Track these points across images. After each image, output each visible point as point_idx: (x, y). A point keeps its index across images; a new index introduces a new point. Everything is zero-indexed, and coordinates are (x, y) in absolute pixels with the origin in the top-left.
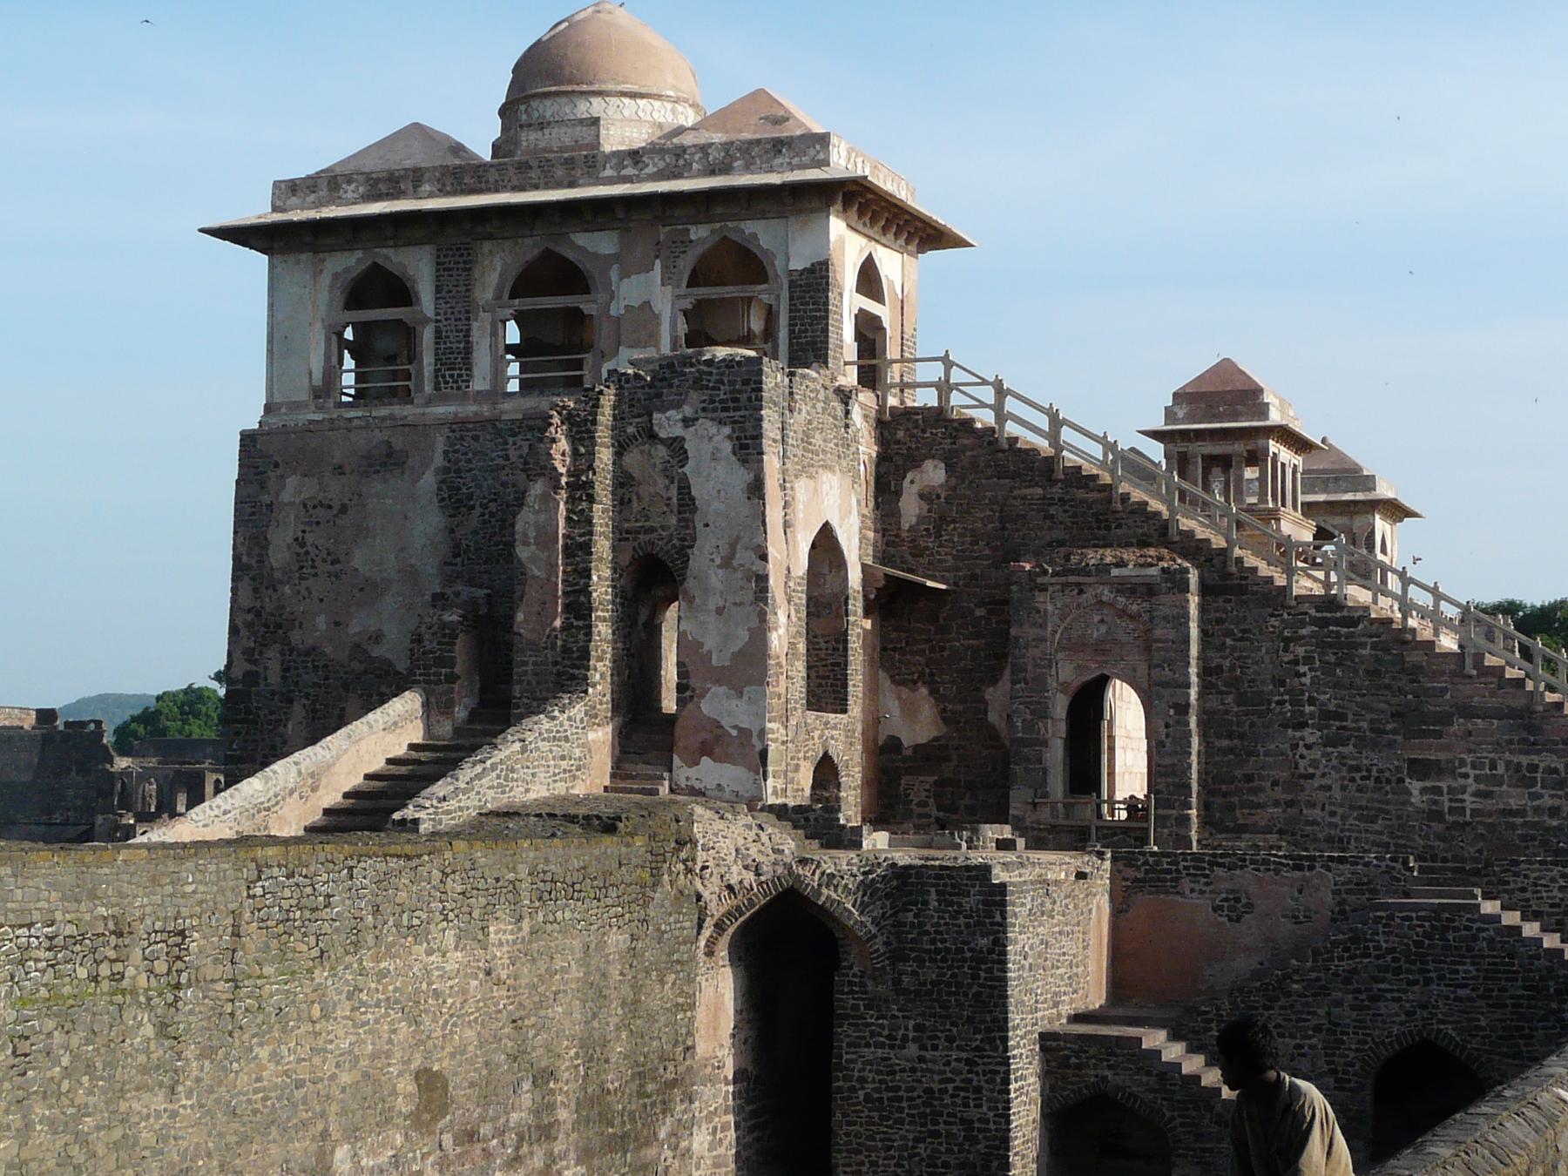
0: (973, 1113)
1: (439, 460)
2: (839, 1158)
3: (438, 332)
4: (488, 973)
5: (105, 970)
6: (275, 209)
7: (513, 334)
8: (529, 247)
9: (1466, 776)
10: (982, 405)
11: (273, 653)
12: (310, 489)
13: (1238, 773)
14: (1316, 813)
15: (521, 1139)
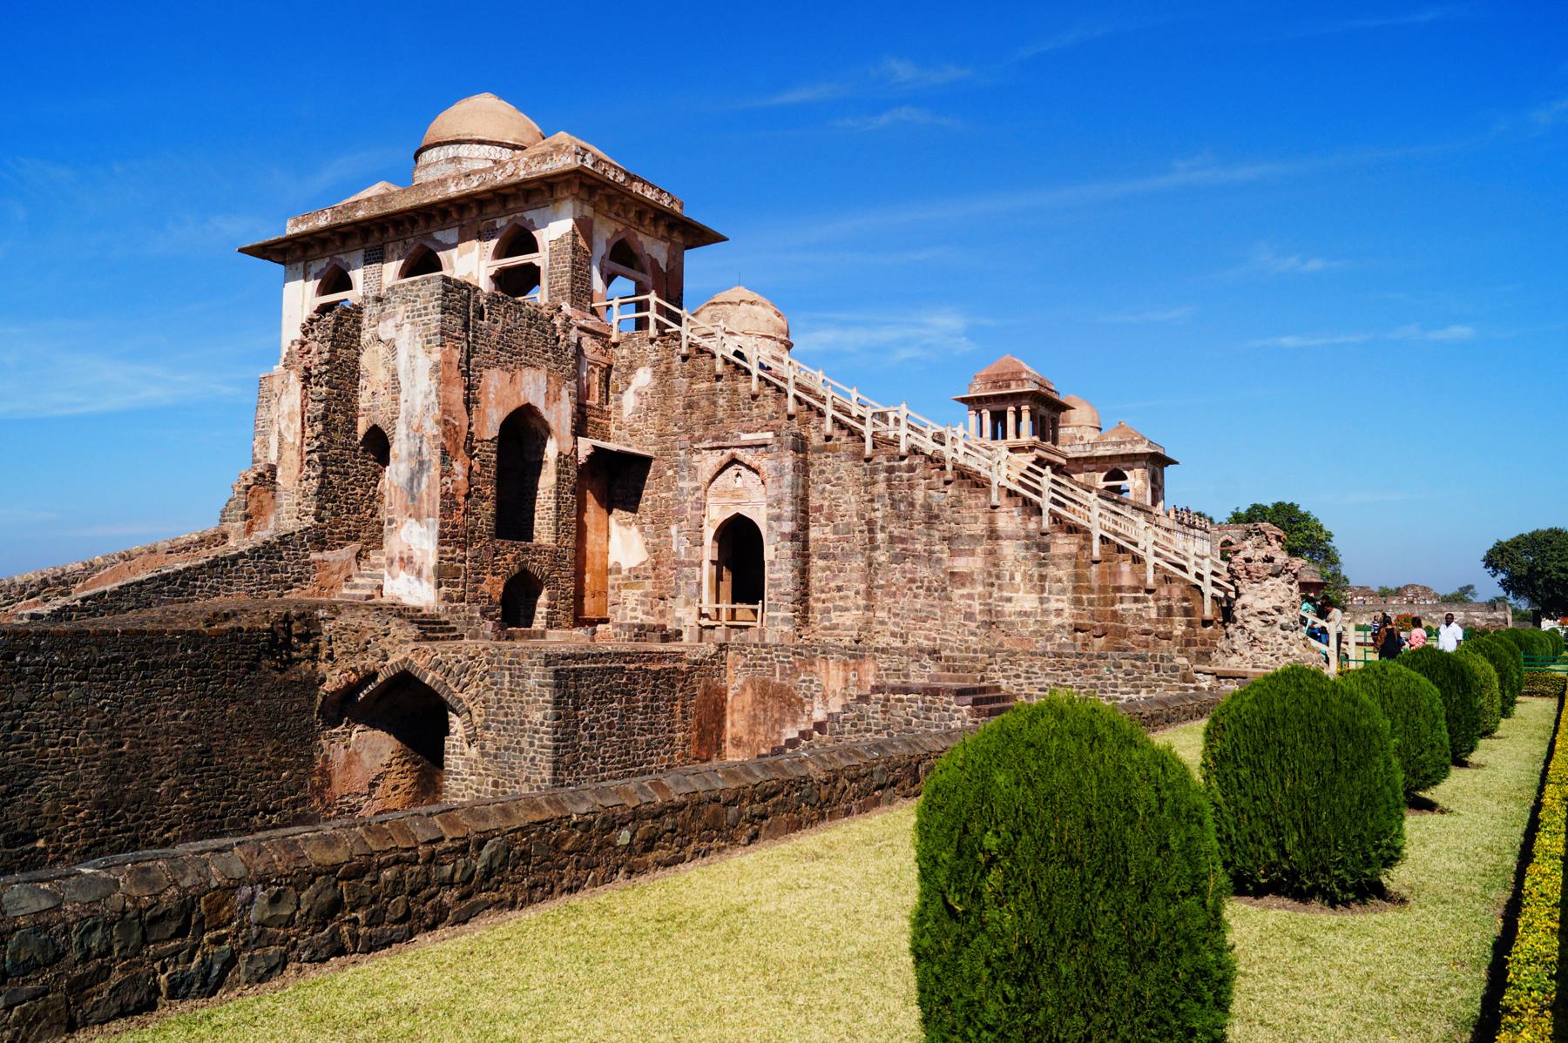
13: (832, 585)
14: (882, 615)
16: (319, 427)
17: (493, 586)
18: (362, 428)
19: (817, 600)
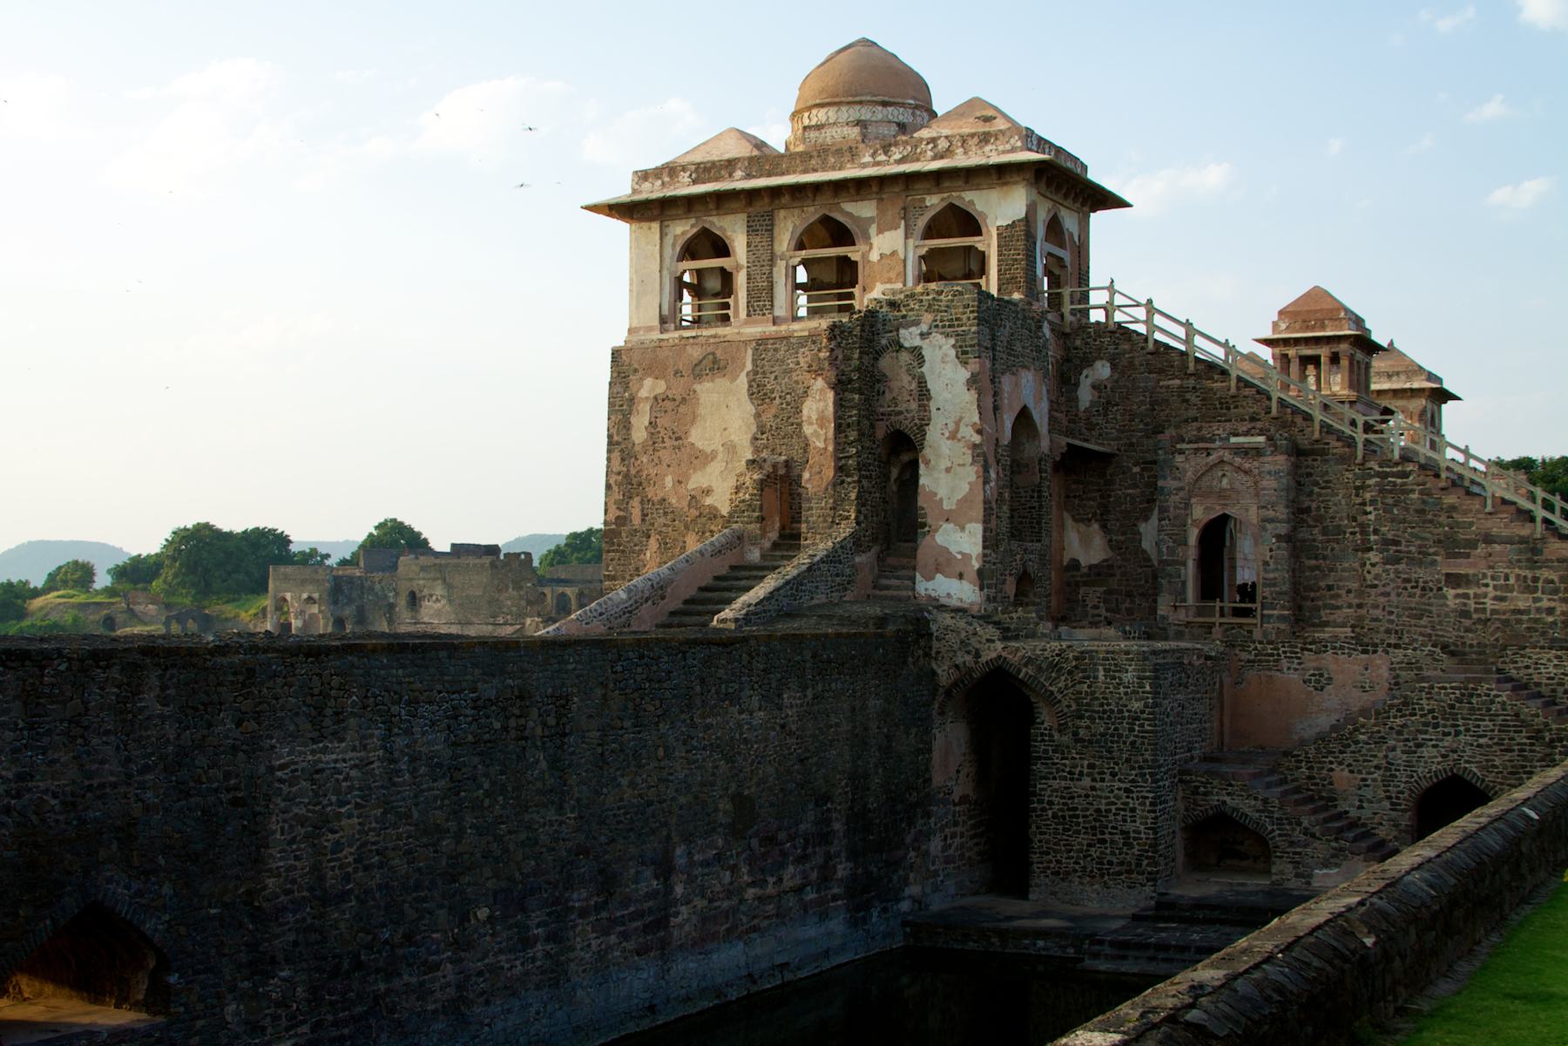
0: (1130, 827)
1: (749, 366)
2: (1035, 858)
3: (748, 274)
4: (783, 727)
5: (512, 723)
6: (634, 191)
7: (802, 276)
8: (812, 213)
9: (1487, 585)
10: (1137, 321)
11: (636, 502)
12: (661, 386)
14: (1378, 613)
15: (807, 841)
16: (853, 435)
17: (1010, 588)
18: (880, 433)
19: (1305, 598)
